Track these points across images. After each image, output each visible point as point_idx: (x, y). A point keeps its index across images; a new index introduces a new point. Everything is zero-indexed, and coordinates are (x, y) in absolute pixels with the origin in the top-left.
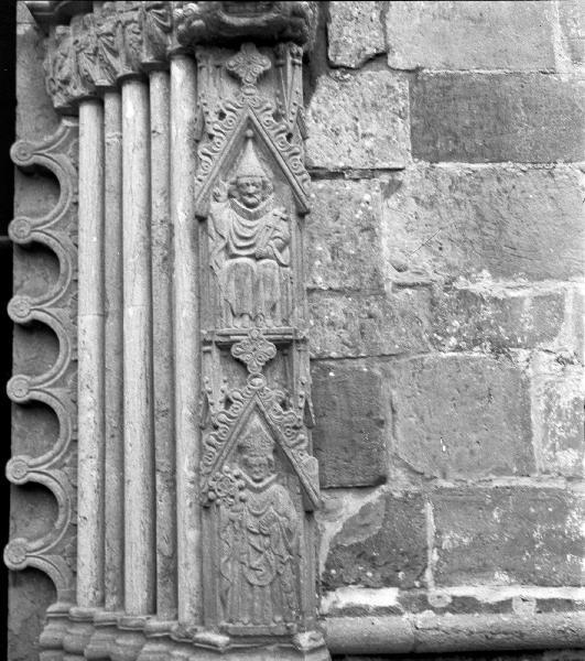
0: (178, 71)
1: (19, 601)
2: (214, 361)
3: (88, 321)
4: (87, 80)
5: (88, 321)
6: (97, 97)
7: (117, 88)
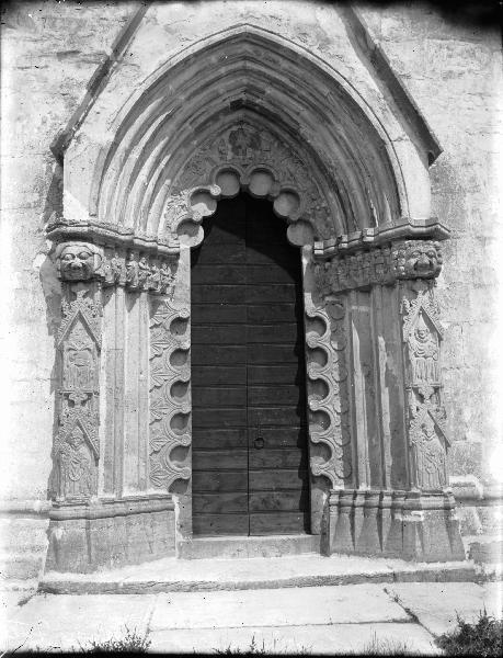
2: (413, 396)
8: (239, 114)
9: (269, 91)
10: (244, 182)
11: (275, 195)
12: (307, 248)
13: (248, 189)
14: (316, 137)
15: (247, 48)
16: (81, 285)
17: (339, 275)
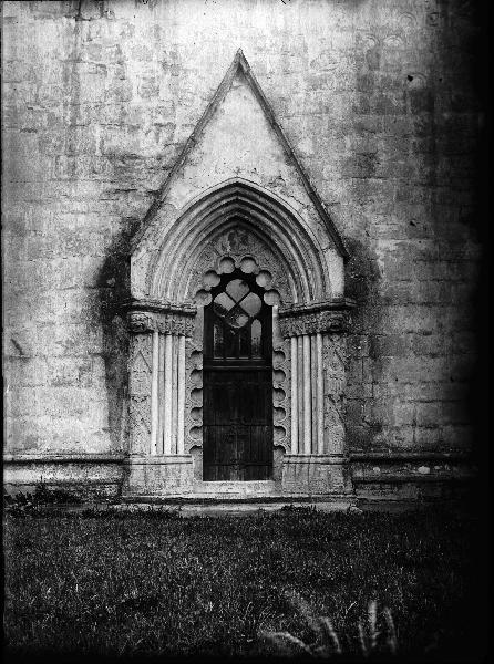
0: (319, 337)
1: (276, 454)
7: (303, 336)
8: (235, 224)
9: (253, 212)
10: (237, 265)
12: (276, 307)
14: (283, 243)
15: (237, 189)
17: (290, 324)
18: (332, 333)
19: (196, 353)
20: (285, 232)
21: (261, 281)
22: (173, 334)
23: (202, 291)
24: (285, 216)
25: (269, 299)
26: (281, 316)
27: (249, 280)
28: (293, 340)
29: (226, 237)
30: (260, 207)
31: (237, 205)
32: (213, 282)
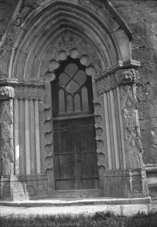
3: (107, 127)
4: (104, 89)
5: (107, 127)
6: (106, 92)
7: (109, 91)
8: (64, 29)
9: (71, 19)
11: (80, 57)
13: (70, 57)
15: (60, 6)
16: (6, 101)
18: (125, 85)
19: (46, 110)
20: (92, 28)
21: (83, 62)
22: (29, 100)
23: (48, 72)
24: (89, 17)
25: (89, 72)
26: (96, 81)
27: (77, 61)
28: (105, 94)
29: (60, 39)
30: (75, 15)
31: (62, 17)
32: (56, 66)
